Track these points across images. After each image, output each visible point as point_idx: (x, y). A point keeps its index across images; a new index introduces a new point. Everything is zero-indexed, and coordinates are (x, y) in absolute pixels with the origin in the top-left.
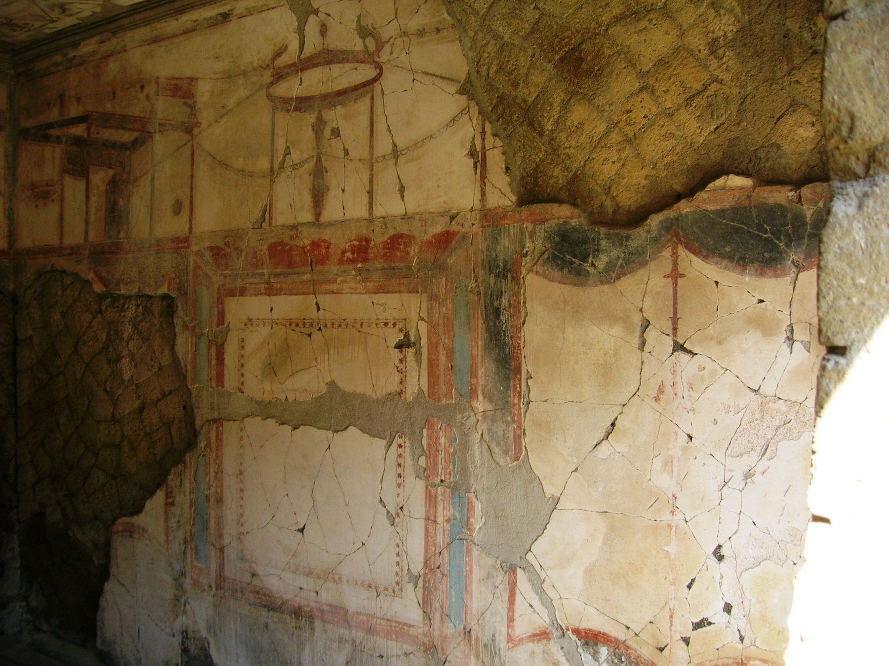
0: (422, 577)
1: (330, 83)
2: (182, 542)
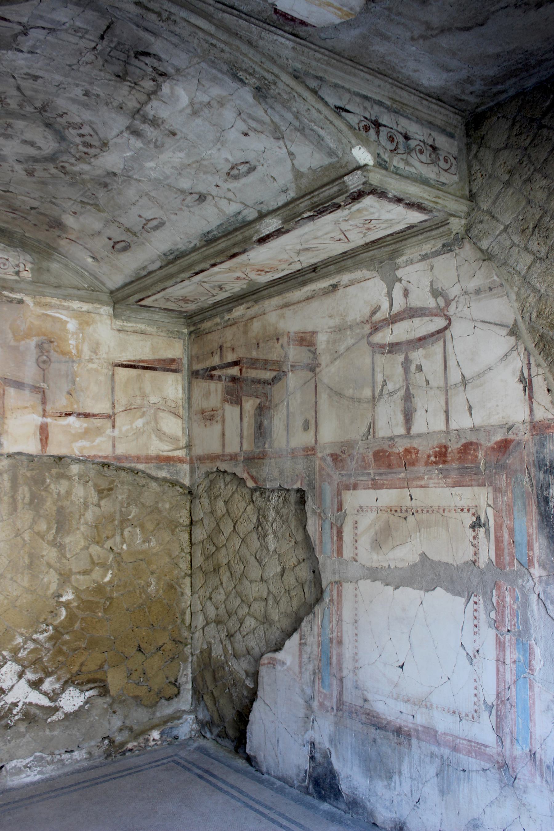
0: (495, 707)
1: (413, 332)
2: (311, 673)
